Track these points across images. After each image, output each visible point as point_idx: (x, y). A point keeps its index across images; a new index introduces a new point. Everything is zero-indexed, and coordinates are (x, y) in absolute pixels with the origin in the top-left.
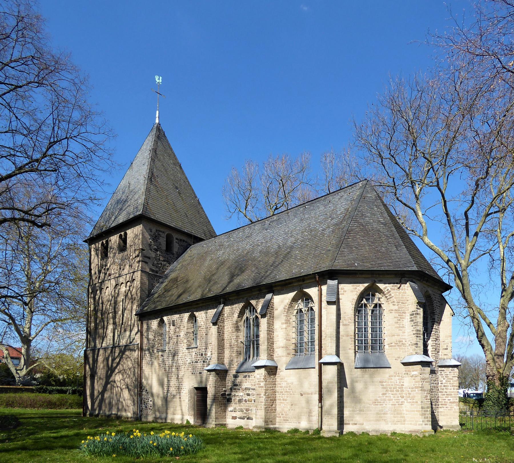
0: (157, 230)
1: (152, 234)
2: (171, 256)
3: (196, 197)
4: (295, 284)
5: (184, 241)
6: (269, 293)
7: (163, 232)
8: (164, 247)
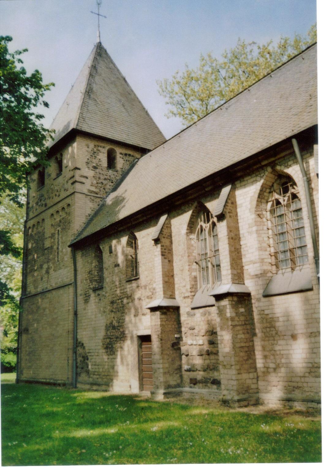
0: (95, 146)
1: (90, 150)
2: (115, 173)
3: (144, 109)
4: (264, 163)
5: (130, 155)
6: (225, 185)
7: (104, 147)
8: (105, 163)
